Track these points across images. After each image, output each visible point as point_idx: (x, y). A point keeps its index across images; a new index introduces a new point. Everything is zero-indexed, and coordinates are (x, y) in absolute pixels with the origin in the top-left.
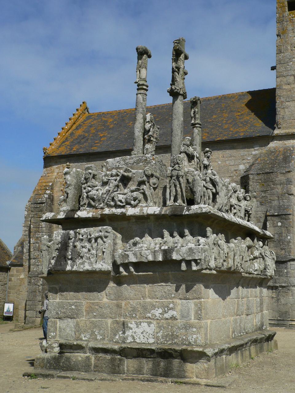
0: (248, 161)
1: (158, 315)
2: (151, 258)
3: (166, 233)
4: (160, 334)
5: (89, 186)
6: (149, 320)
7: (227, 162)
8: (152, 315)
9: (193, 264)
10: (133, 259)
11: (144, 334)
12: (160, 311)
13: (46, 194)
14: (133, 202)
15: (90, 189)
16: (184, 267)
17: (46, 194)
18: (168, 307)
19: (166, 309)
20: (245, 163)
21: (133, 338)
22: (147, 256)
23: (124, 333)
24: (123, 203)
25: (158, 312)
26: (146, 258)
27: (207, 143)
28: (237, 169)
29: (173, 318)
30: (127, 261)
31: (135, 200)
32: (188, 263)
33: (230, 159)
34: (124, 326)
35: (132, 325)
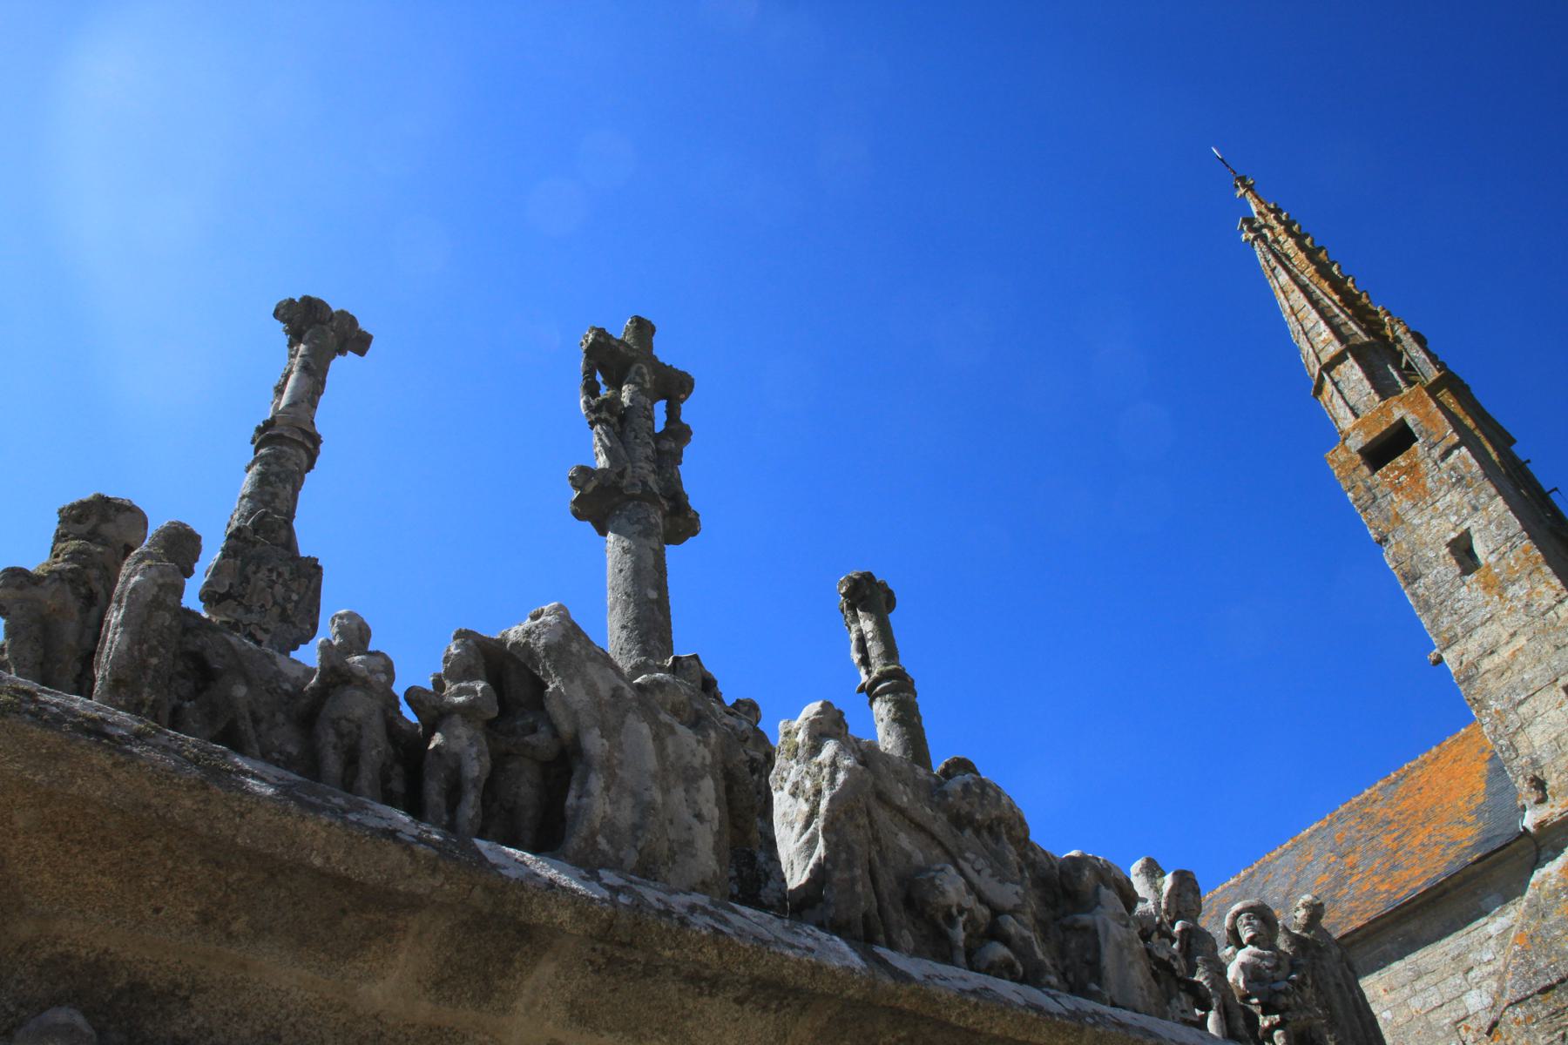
0: (1490, 968)
7: (1416, 1003)
20: (1483, 978)
28: (1462, 1013)
33: (1418, 985)
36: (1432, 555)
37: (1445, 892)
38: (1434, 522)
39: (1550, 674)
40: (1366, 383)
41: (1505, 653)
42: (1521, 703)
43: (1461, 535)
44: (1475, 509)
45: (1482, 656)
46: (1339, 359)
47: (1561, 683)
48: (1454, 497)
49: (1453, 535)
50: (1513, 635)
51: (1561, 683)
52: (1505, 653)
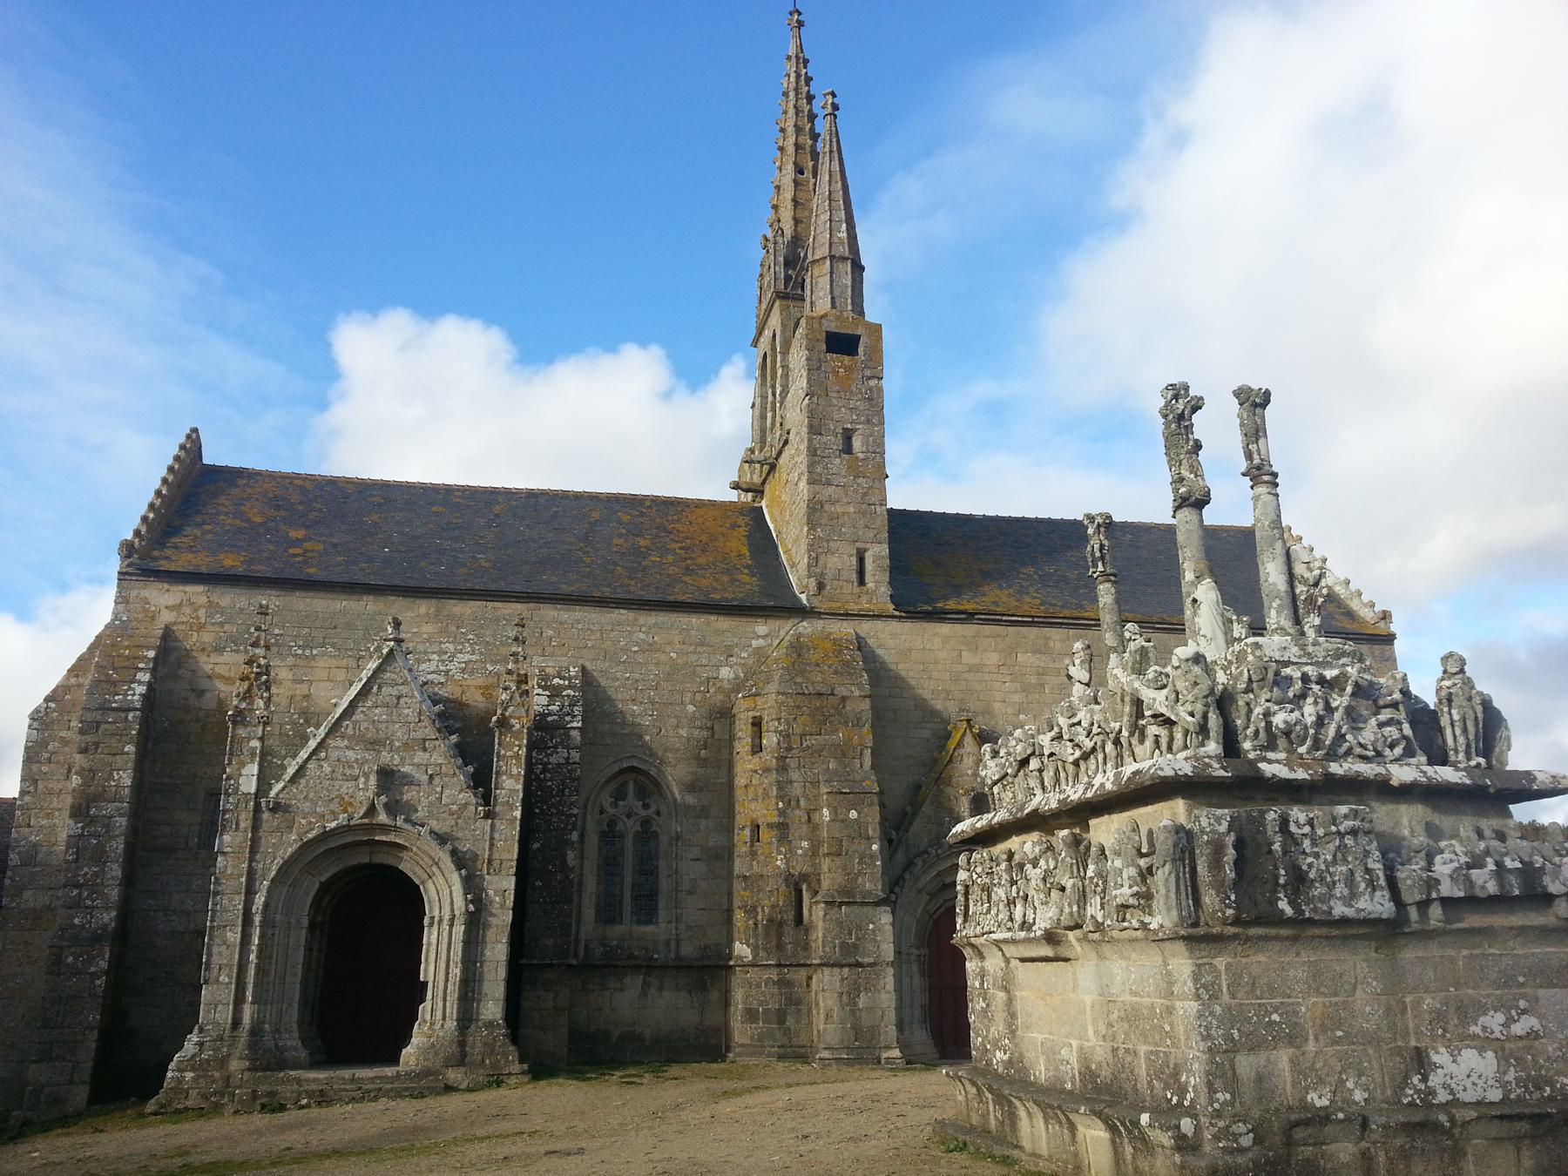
1: (1497, 1029)
2: (1492, 888)
4: (1511, 1076)
6: (1484, 1043)
7: (694, 658)
8: (1484, 1029)
11: (1474, 1078)
12: (1500, 1017)
13: (140, 683)
17: (140, 683)
18: (1517, 1007)
19: (1513, 1012)
21: (1452, 1092)
23: (1425, 1079)
25: (1494, 1021)
26: (1483, 887)
29: (1532, 1035)
34: (1420, 1061)
35: (1440, 1057)
44: (868, 422)
52: (839, 509)
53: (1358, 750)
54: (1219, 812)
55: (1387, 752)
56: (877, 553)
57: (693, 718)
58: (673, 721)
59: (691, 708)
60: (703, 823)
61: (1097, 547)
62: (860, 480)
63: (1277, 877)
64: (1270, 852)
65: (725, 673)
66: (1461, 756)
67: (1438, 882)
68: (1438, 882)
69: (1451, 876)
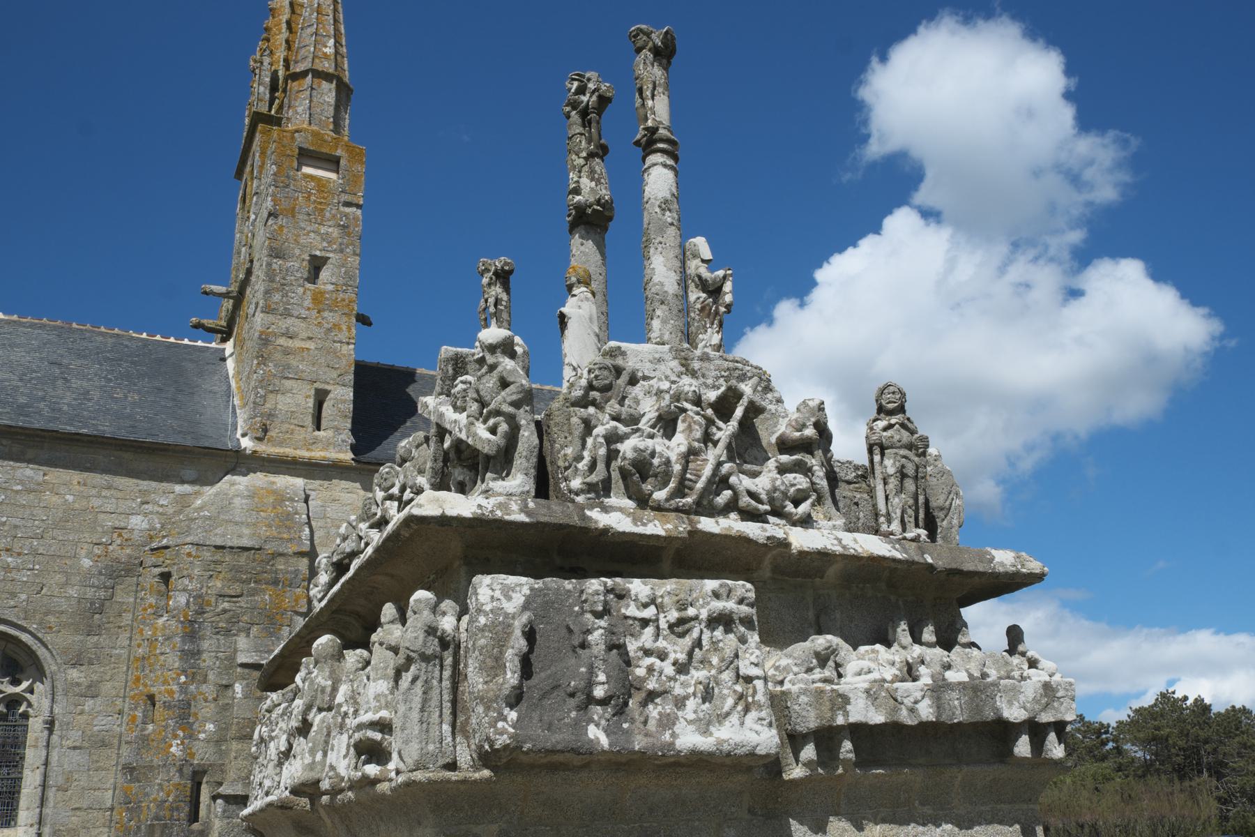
2: (926, 711)
3: (903, 631)
5: (616, 418)
7: (95, 502)
9: (1052, 736)
10: (862, 712)
14: (790, 507)
15: (622, 429)
16: (1023, 747)
20: (151, 513)
22: (916, 702)
24: (760, 501)
26: (912, 710)
27: (37, 436)
28: (123, 525)
30: (840, 720)
31: (797, 503)
32: (1037, 731)
36: (297, 252)
37: (165, 450)
38: (312, 235)
39: (314, 376)
40: (332, 109)
41: (297, 344)
42: (287, 378)
43: (322, 258)
44: (342, 251)
45: (283, 335)
46: (327, 77)
47: (316, 385)
48: (335, 232)
49: (318, 253)
50: (310, 338)
51: (316, 385)
52: (297, 344)
53: (745, 501)
54: (512, 580)
55: (790, 507)
56: (342, 396)
57: (89, 574)
58: (60, 578)
59: (87, 563)
60: (89, 704)
61: (492, 300)
62: (326, 314)
63: (590, 684)
64: (584, 645)
65: (138, 522)
66: (895, 526)
67: (846, 700)
68: (846, 700)
69: (867, 691)
